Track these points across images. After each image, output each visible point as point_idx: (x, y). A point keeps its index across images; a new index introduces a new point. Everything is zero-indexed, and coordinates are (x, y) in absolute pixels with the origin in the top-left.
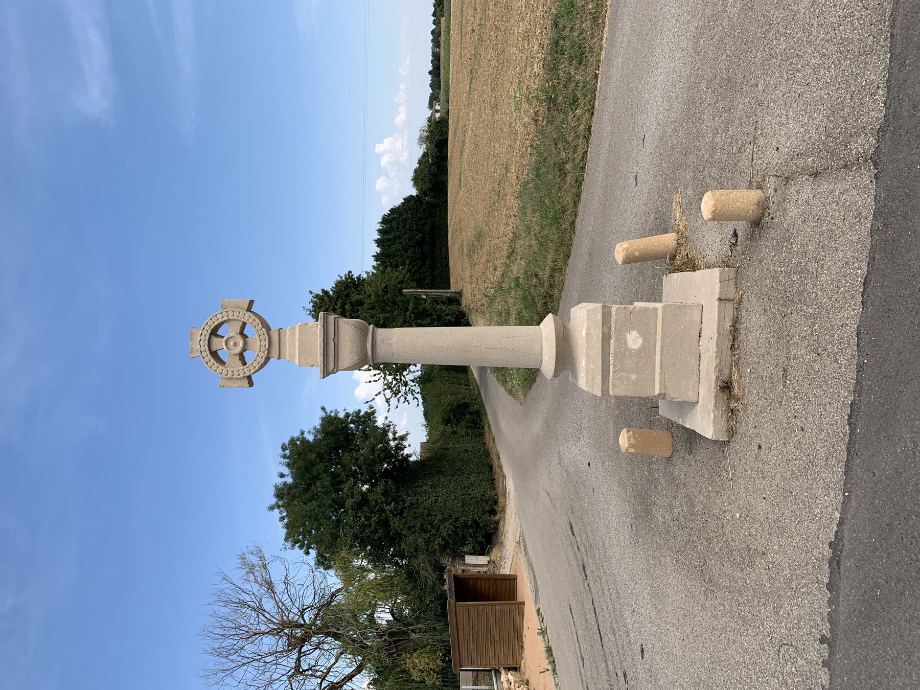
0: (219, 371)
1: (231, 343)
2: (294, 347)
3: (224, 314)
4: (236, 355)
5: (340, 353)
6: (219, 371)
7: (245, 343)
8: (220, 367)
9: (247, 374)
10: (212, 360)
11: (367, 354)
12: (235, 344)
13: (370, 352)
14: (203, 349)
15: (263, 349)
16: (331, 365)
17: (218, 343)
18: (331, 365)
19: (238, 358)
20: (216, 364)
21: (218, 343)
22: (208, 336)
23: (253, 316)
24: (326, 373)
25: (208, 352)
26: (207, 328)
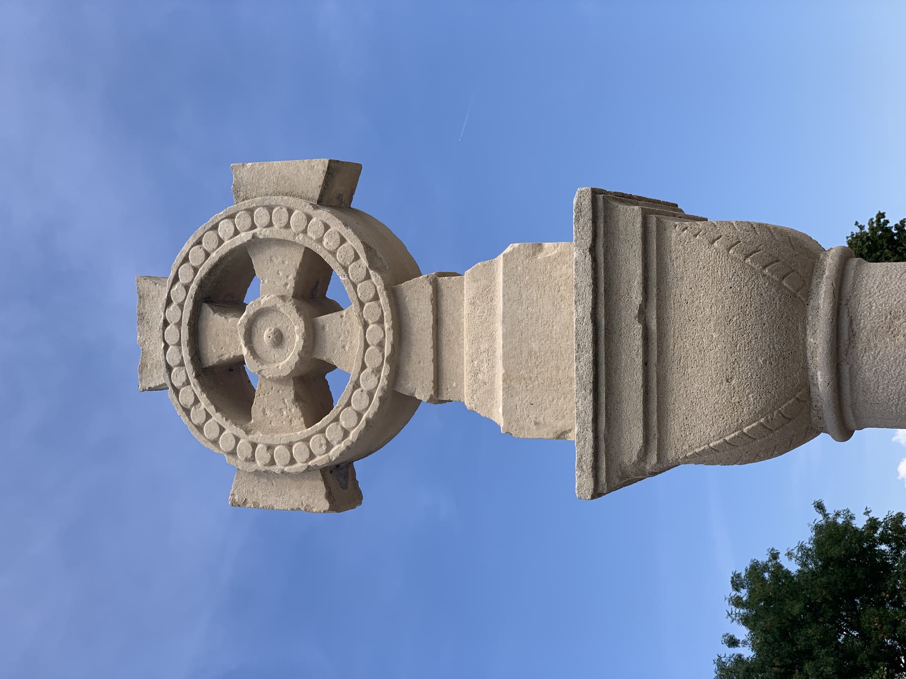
0: (226, 443)
1: (265, 335)
2: (491, 351)
3: (242, 221)
4: (280, 380)
5: (675, 379)
6: (226, 443)
7: (313, 336)
8: (231, 430)
9: (320, 460)
10: (203, 398)
11: (806, 384)
12: (279, 339)
13: (821, 378)
14: (173, 356)
15: (374, 358)
16: (632, 438)
17: (225, 336)
18: (632, 438)
19: (289, 393)
20: (217, 417)
21: (225, 336)
22: (189, 305)
23: (337, 226)
24: (611, 474)
25: (189, 367)
26: (186, 274)
